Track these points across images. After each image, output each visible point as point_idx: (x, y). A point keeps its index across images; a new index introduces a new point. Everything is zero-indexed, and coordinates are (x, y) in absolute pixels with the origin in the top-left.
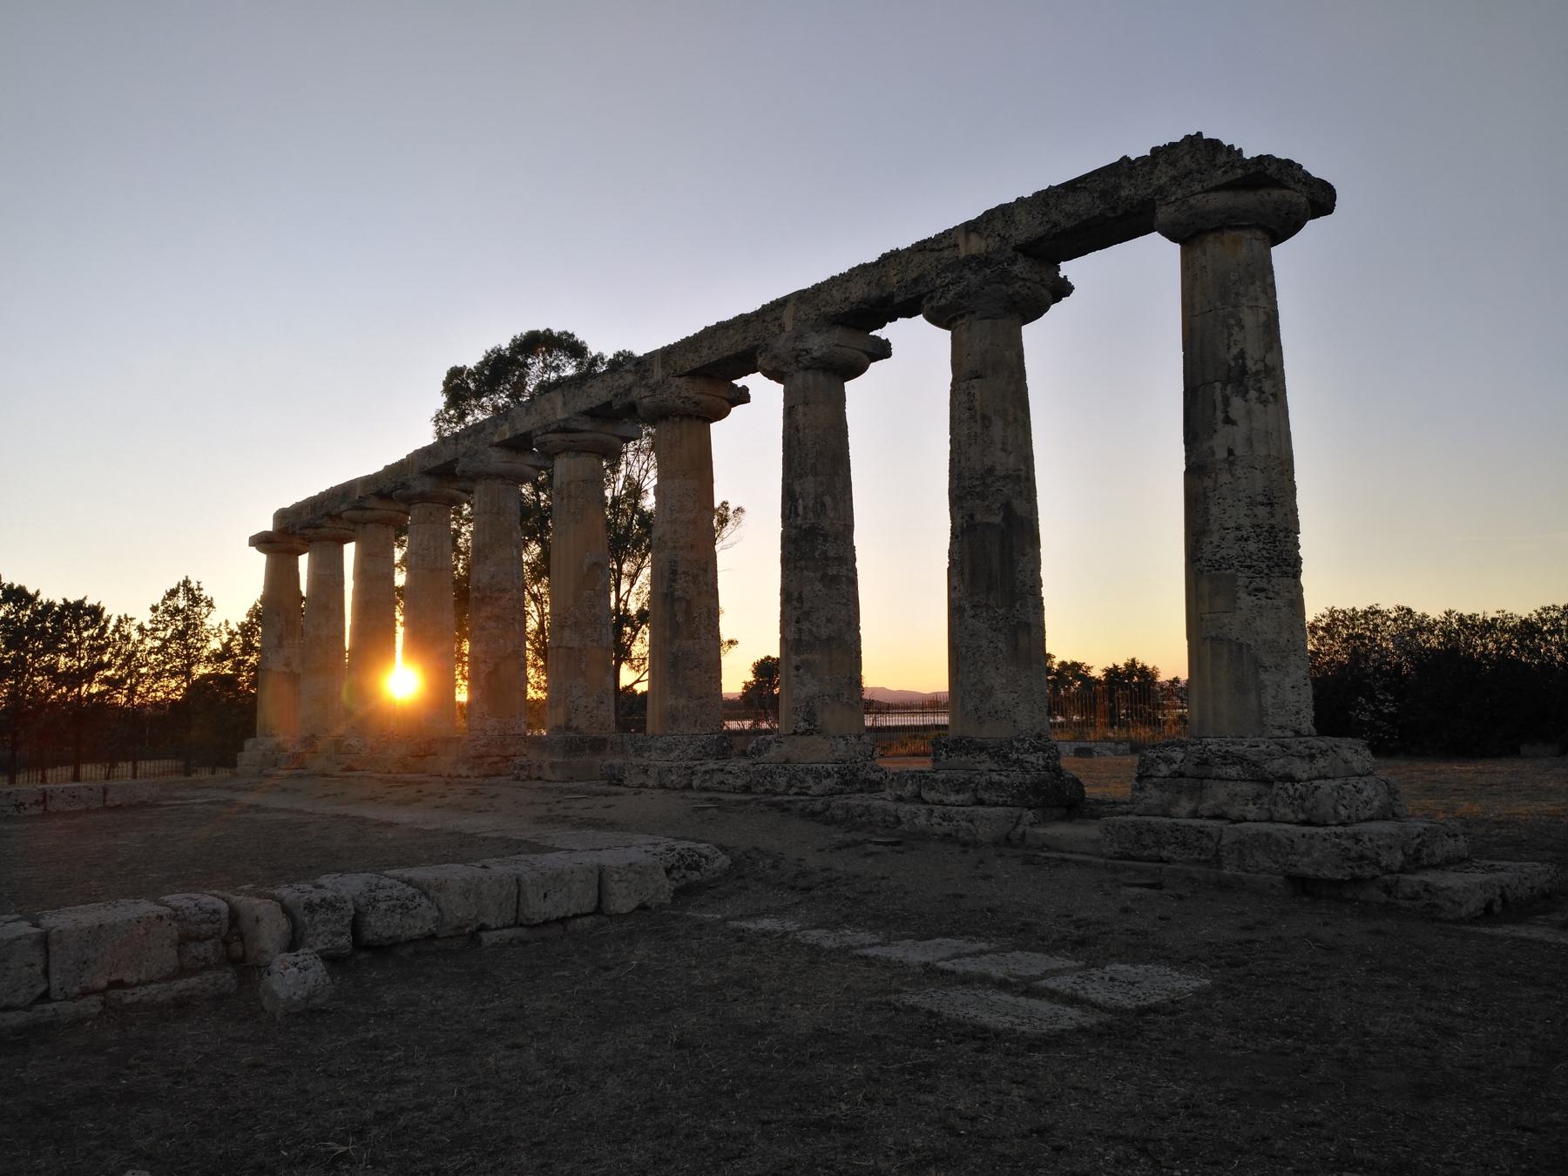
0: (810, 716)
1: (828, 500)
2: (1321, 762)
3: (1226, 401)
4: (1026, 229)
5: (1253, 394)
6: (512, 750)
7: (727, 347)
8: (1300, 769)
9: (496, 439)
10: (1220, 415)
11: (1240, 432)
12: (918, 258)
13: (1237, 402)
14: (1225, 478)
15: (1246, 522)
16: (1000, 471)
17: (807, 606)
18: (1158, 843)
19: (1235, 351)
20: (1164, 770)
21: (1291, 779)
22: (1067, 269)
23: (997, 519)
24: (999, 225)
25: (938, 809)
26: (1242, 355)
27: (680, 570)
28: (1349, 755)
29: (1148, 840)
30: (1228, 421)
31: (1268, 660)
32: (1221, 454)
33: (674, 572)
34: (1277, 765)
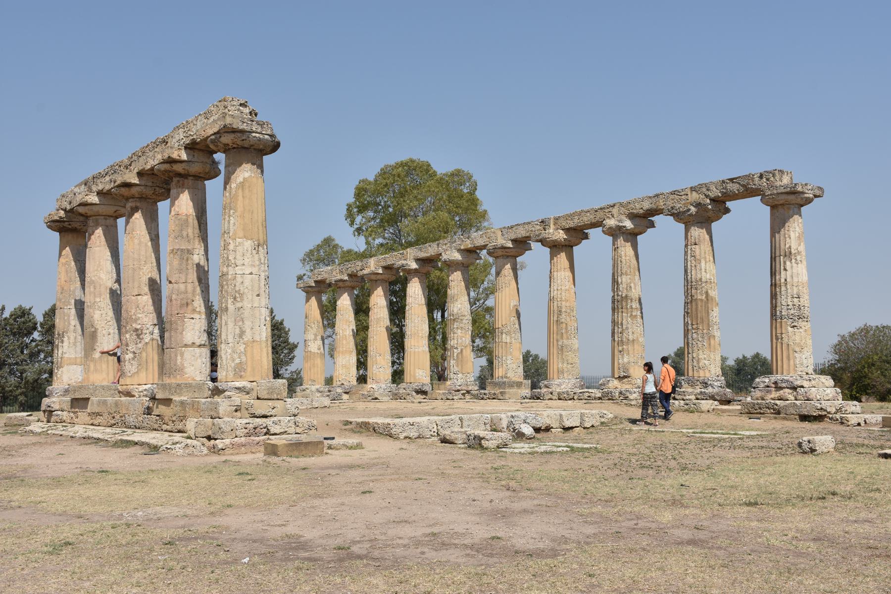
0: (626, 370)
1: (632, 285)
2: (813, 382)
3: (785, 263)
4: (715, 192)
5: (793, 261)
6: (470, 388)
7: (587, 219)
8: (805, 384)
9: (462, 247)
10: (782, 268)
11: (789, 273)
12: (672, 197)
13: (788, 263)
14: (783, 288)
15: (790, 303)
16: (704, 280)
17: (624, 327)
18: (760, 408)
19: (787, 246)
20: (762, 385)
21: (802, 387)
22: (729, 204)
23: (704, 297)
24: (704, 190)
25: (682, 402)
26: (790, 247)
27: (563, 310)
28: (824, 381)
29: (757, 407)
30: (785, 270)
31: (797, 349)
32: (783, 280)
33: (560, 311)
34: (798, 383)
